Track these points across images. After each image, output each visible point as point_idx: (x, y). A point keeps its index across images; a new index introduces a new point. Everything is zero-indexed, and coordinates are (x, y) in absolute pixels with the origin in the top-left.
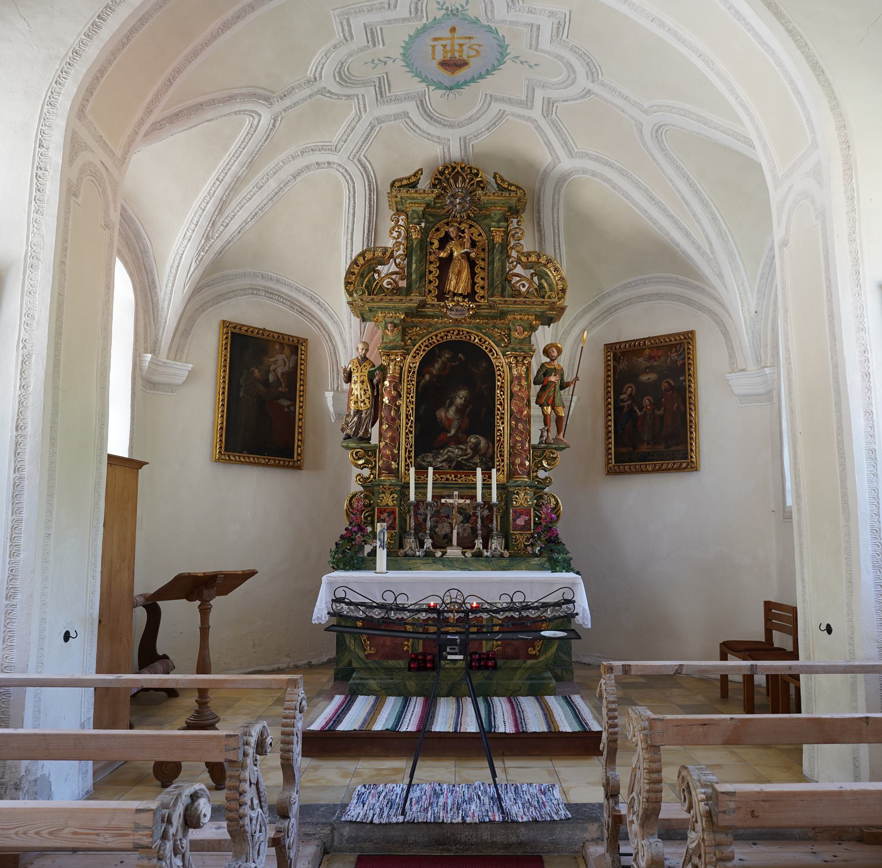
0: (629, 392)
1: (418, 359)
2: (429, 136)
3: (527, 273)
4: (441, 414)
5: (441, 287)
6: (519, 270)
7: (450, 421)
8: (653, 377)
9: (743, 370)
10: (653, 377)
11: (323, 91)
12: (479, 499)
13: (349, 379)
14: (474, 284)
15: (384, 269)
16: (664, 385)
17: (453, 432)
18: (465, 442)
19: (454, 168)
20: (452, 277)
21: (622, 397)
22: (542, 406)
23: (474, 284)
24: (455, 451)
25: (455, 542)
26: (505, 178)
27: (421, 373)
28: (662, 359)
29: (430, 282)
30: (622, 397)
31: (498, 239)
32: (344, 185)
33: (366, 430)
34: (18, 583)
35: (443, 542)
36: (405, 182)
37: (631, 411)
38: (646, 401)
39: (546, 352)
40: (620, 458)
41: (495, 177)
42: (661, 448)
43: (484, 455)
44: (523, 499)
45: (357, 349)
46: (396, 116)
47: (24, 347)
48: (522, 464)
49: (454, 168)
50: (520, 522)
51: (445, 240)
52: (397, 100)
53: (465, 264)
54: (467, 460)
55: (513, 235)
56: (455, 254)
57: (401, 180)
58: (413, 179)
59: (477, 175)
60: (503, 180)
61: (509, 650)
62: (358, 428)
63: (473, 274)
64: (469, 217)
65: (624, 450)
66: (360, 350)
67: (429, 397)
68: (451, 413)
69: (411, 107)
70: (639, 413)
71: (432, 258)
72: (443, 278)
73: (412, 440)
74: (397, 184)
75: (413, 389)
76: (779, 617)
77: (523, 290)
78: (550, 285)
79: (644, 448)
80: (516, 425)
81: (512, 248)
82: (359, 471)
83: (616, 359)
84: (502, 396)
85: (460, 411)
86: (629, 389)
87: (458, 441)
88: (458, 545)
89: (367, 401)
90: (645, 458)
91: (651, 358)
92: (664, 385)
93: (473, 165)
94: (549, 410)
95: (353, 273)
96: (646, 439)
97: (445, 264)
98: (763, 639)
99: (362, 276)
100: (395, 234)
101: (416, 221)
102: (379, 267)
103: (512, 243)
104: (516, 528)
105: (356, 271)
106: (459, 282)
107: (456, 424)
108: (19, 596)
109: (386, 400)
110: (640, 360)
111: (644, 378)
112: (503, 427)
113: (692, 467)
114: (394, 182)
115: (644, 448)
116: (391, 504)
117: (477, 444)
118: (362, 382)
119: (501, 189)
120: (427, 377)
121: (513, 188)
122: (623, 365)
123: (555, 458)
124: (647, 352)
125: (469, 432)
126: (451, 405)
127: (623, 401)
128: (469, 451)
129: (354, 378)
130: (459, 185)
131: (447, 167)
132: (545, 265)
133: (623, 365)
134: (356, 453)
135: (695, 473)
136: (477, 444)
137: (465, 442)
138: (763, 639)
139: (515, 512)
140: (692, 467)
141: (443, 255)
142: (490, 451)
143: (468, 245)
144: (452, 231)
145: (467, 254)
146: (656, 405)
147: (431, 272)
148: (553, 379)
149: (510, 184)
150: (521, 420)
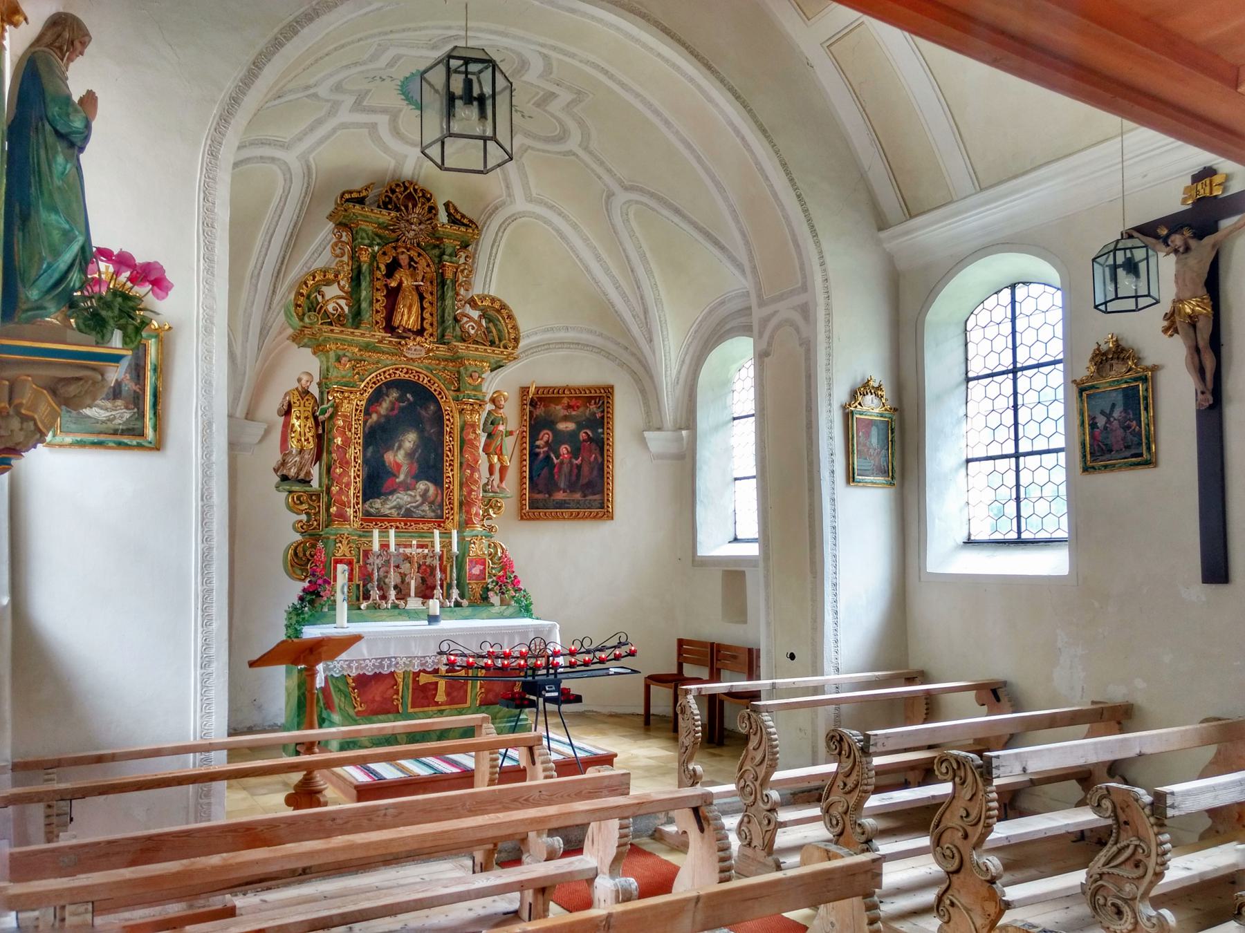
0: (545, 438)
1: (366, 395)
2: (386, 149)
3: (475, 314)
4: (389, 457)
5: (389, 318)
6: (468, 310)
7: (399, 466)
8: (571, 426)
9: (659, 429)
10: (571, 426)
11: (315, 95)
12: (438, 549)
13: (287, 413)
14: (423, 319)
15: (332, 291)
16: (582, 436)
17: (402, 477)
18: (414, 489)
19: (406, 188)
20: (402, 309)
21: (538, 443)
22: (488, 454)
23: (423, 319)
24: (402, 498)
25: (413, 594)
26: (460, 209)
27: (368, 413)
28: (581, 409)
29: (377, 312)
30: (538, 443)
31: (449, 275)
32: (281, 182)
33: (308, 473)
34: (213, 651)
35: (402, 594)
36: (355, 195)
37: (548, 458)
38: (564, 449)
39: (493, 401)
40: (534, 505)
41: (447, 205)
42: (578, 496)
43: (432, 503)
44: (475, 550)
45: (299, 380)
46: (365, 125)
47: (203, 414)
48: (477, 514)
49: (406, 188)
50: (476, 570)
51: (393, 267)
52: (372, 110)
53: (416, 298)
54: (416, 507)
55: (462, 271)
56: (405, 284)
57: (351, 192)
58: (364, 193)
59: (429, 200)
60: (456, 210)
61: (491, 696)
62: (300, 470)
63: (423, 309)
64: (418, 244)
65: (540, 496)
66: (303, 382)
67: (379, 437)
68: (400, 457)
69: (383, 120)
70: (555, 461)
71: (378, 285)
72: (391, 310)
73: (360, 485)
74: (347, 196)
75: (360, 429)
76: (687, 651)
77: (472, 332)
78: (499, 331)
79: (560, 496)
80: (472, 474)
81: (460, 285)
82: (296, 518)
83: (533, 403)
84: (451, 443)
85: (410, 455)
86: (546, 436)
87: (407, 487)
88: (416, 596)
89: (311, 439)
90: (561, 505)
91: (569, 407)
92: (582, 436)
93: (421, 184)
94: (495, 459)
95: (302, 295)
96: (562, 486)
97: (393, 295)
98: (675, 671)
99: (308, 297)
100: (338, 251)
101: (367, 242)
102: (324, 289)
103: (461, 279)
104: (472, 577)
105: (305, 292)
106: (407, 317)
107: (404, 469)
108: (214, 665)
109: (339, 441)
110: (558, 407)
111: (562, 426)
112: (453, 475)
113: (609, 516)
114: (343, 194)
115: (560, 496)
116: (347, 554)
117: (427, 491)
118: (307, 418)
119: (453, 220)
120: (375, 417)
121: (465, 221)
122: (540, 411)
123: (500, 508)
124: (565, 401)
125: (418, 478)
126: (400, 447)
127: (538, 447)
128: (418, 498)
129: (295, 412)
130: (417, 210)
131: (398, 185)
132: (498, 311)
133: (540, 411)
134: (298, 498)
135: (609, 523)
136: (427, 491)
137: (414, 489)
138: (675, 671)
139: (471, 561)
140: (609, 516)
141: (394, 284)
142: (439, 498)
143: (420, 278)
144: (404, 259)
145: (417, 287)
146: (575, 453)
147: (378, 301)
148: (501, 428)
149: (463, 216)
150: (469, 466)
